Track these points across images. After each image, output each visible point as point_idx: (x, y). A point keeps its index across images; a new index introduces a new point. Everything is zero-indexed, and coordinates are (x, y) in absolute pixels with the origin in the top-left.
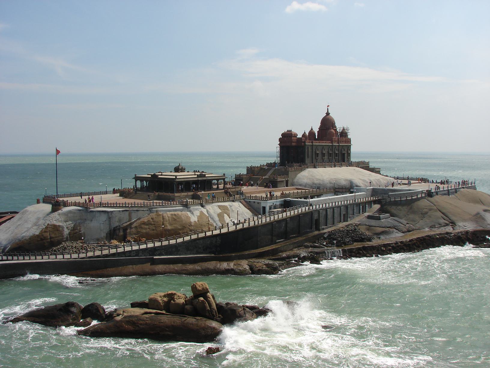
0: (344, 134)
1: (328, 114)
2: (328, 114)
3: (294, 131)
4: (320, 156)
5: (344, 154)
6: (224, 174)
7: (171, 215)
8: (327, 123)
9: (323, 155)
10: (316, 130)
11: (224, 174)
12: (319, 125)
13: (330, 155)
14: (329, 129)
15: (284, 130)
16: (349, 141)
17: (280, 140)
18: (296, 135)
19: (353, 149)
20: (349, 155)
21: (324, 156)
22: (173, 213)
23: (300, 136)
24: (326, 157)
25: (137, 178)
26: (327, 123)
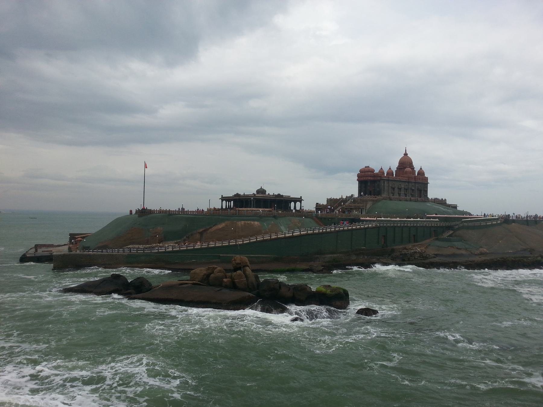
4: (396, 190)
7: (245, 223)
10: (394, 169)
13: (406, 190)
16: (427, 179)
18: (373, 171)
20: (426, 191)
22: (247, 222)
23: (376, 171)
24: (402, 192)
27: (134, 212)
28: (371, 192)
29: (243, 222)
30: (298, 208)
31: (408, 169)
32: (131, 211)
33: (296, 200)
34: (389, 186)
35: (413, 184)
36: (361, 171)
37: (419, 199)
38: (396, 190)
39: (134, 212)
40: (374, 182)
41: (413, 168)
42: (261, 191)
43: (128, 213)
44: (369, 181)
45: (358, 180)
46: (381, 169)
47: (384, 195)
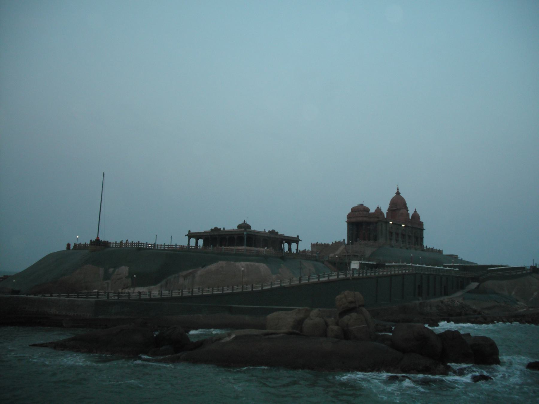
0: (416, 216)
1: (398, 193)
2: (398, 193)
6: (298, 236)
7: (247, 265)
8: (398, 204)
10: (385, 210)
11: (298, 236)
12: (388, 206)
14: (400, 209)
16: (422, 224)
18: (367, 210)
19: (425, 234)
20: (422, 238)
22: (248, 263)
23: (372, 211)
25: (191, 235)
27: (72, 247)
29: (242, 263)
30: (294, 250)
31: (403, 211)
32: (69, 245)
33: (290, 240)
36: (354, 210)
39: (72, 247)
40: (368, 223)
42: (245, 226)
43: (64, 248)
44: (361, 223)
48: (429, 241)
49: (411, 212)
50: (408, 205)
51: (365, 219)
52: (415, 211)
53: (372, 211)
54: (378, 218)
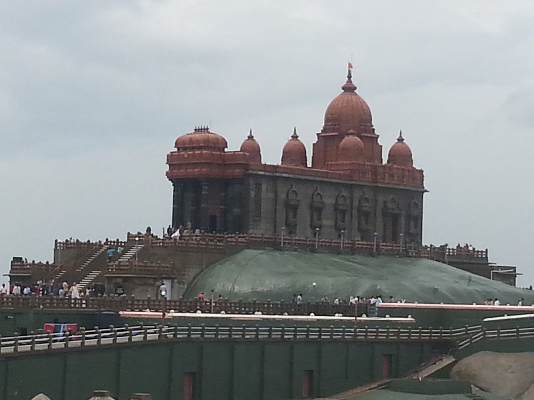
0: (402, 155)
1: (349, 89)
2: (349, 89)
3: (217, 130)
4: (304, 213)
5: (395, 218)
9: (317, 210)
10: (309, 141)
12: (319, 125)
13: (340, 212)
15: (187, 130)
17: (171, 159)
18: (220, 144)
19: (430, 205)
20: (416, 220)
21: (319, 219)
23: (234, 146)
24: (327, 222)
26: (348, 120)
28: (213, 218)
34: (276, 199)
35: (369, 194)
37: (385, 247)
38: (304, 213)
40: (225, 183)
41: (371, 139)
45: (169, 175)
46: (251, 137)
47: (260, 230)
48: (438, 228)
49: (386, 143)
50: (378, 124)
51: (216, 172)
52: (400, 140)
53: (234, 146)
54: (246, 166)
